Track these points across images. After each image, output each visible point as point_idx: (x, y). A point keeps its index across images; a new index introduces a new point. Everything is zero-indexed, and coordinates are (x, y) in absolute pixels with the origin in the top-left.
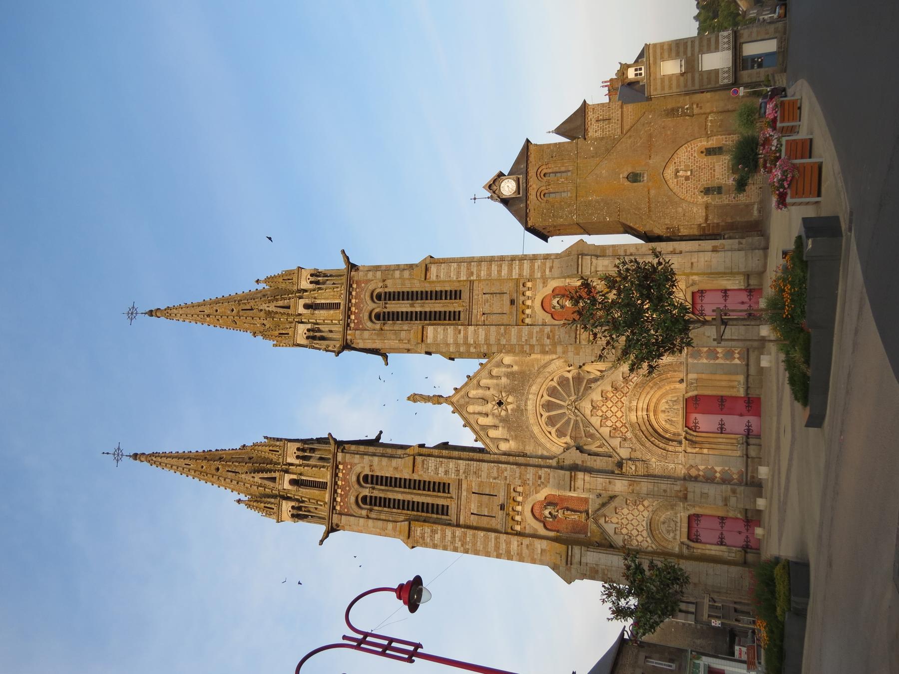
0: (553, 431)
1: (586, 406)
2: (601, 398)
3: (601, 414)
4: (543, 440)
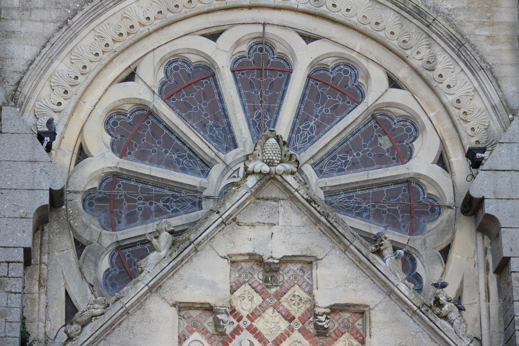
0: (143, 91)
1: (282, 233)
2: (324, 300)
3: (244, 307)
4: (86, 41)
